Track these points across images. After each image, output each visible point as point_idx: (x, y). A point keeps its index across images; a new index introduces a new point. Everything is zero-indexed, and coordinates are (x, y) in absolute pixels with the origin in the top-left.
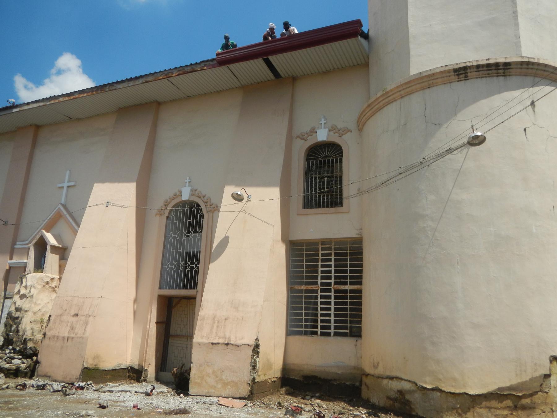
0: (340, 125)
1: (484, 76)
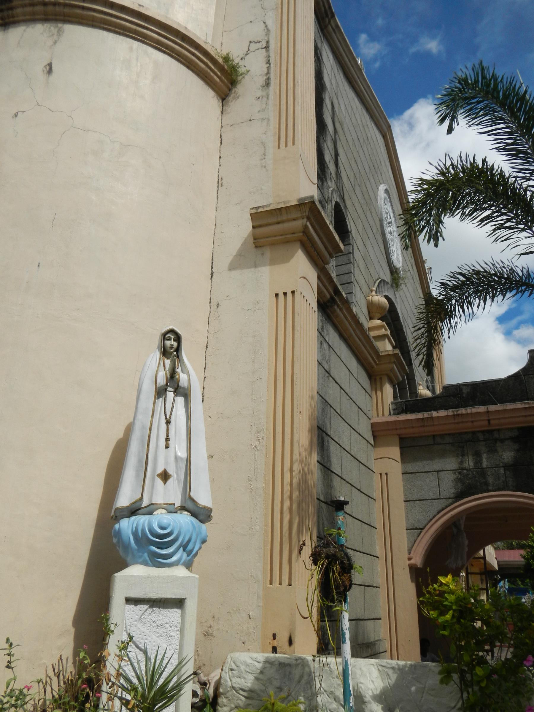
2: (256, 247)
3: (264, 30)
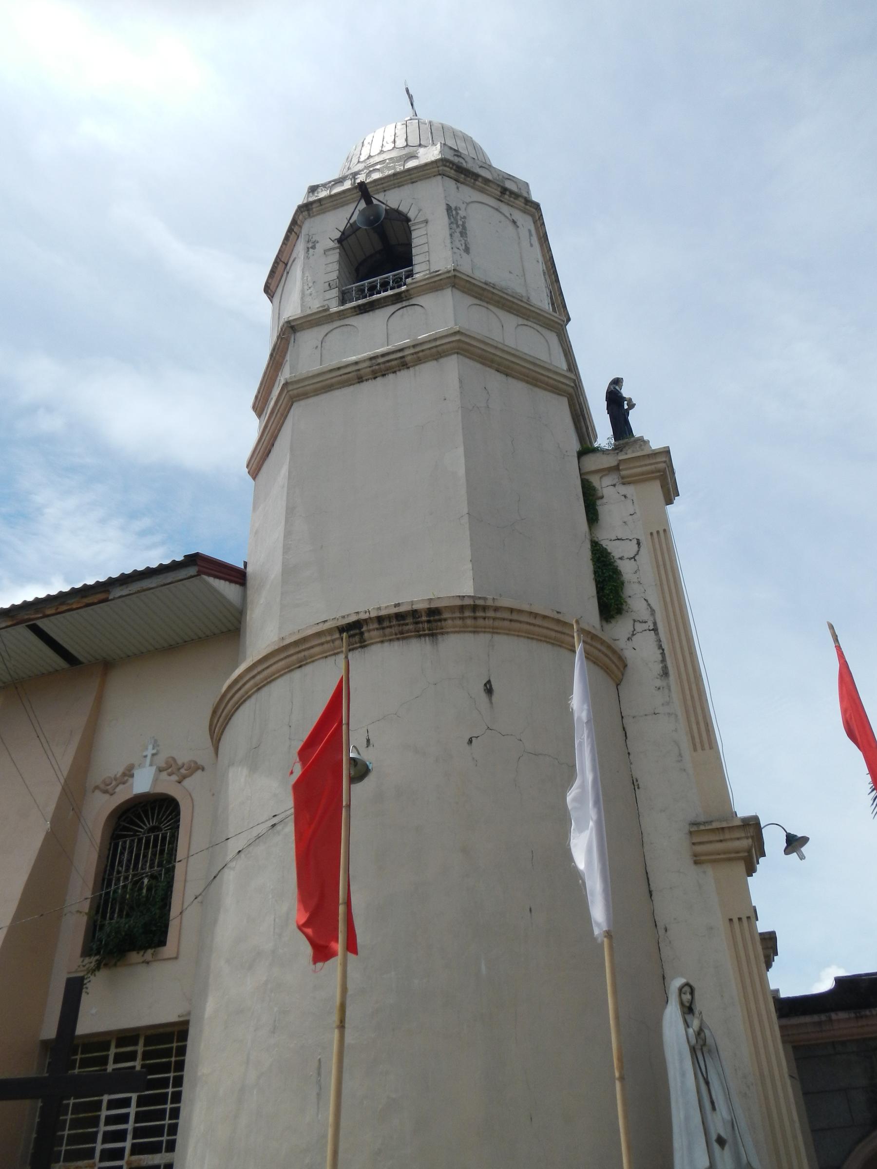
0: (183, 758)
1: (394, 637)
2: (696, 863)
3: (648, 608)
